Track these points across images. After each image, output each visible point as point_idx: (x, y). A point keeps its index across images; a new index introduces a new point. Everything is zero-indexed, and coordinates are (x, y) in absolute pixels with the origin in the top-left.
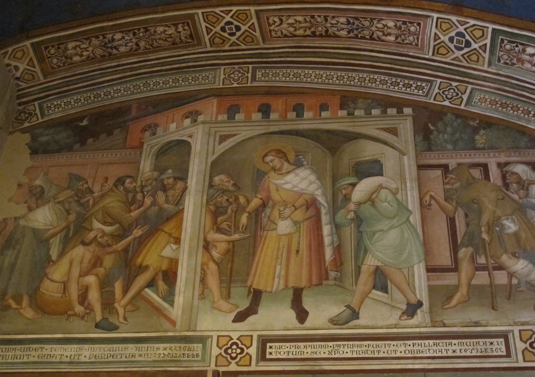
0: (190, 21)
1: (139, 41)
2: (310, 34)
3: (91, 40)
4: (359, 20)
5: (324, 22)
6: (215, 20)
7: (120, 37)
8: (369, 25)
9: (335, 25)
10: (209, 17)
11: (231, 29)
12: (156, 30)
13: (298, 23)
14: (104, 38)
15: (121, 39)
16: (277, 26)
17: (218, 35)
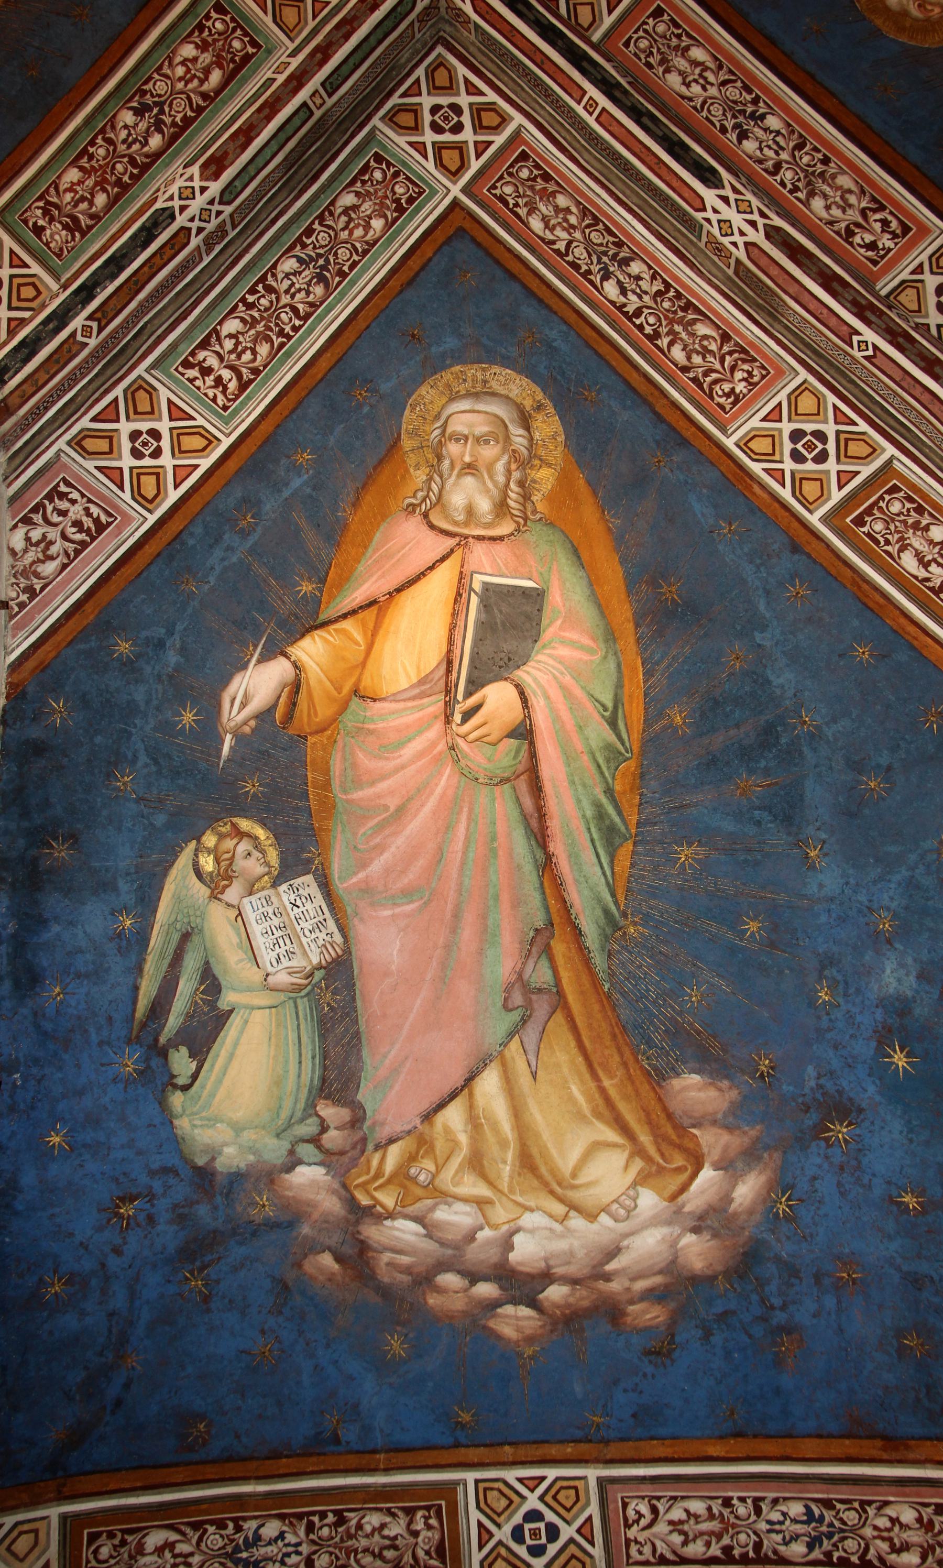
0: (443, 1503)
1: (315, 1552)
2: (718, 1553)
3: (206, 1531)
4: (833, 1507)
5: (753, 1518)
6: (504, 1502)
7: (275, 1533)
8: (856, 1521)
9: (777, 1527)
10: (492, 1495)
11: (535, 1534)
12: (363, 1521)
13: (692, 1521)
14: (238, 1529)
15: (276, 1540)
16: (644, 1529)
17: (503, 1551)
